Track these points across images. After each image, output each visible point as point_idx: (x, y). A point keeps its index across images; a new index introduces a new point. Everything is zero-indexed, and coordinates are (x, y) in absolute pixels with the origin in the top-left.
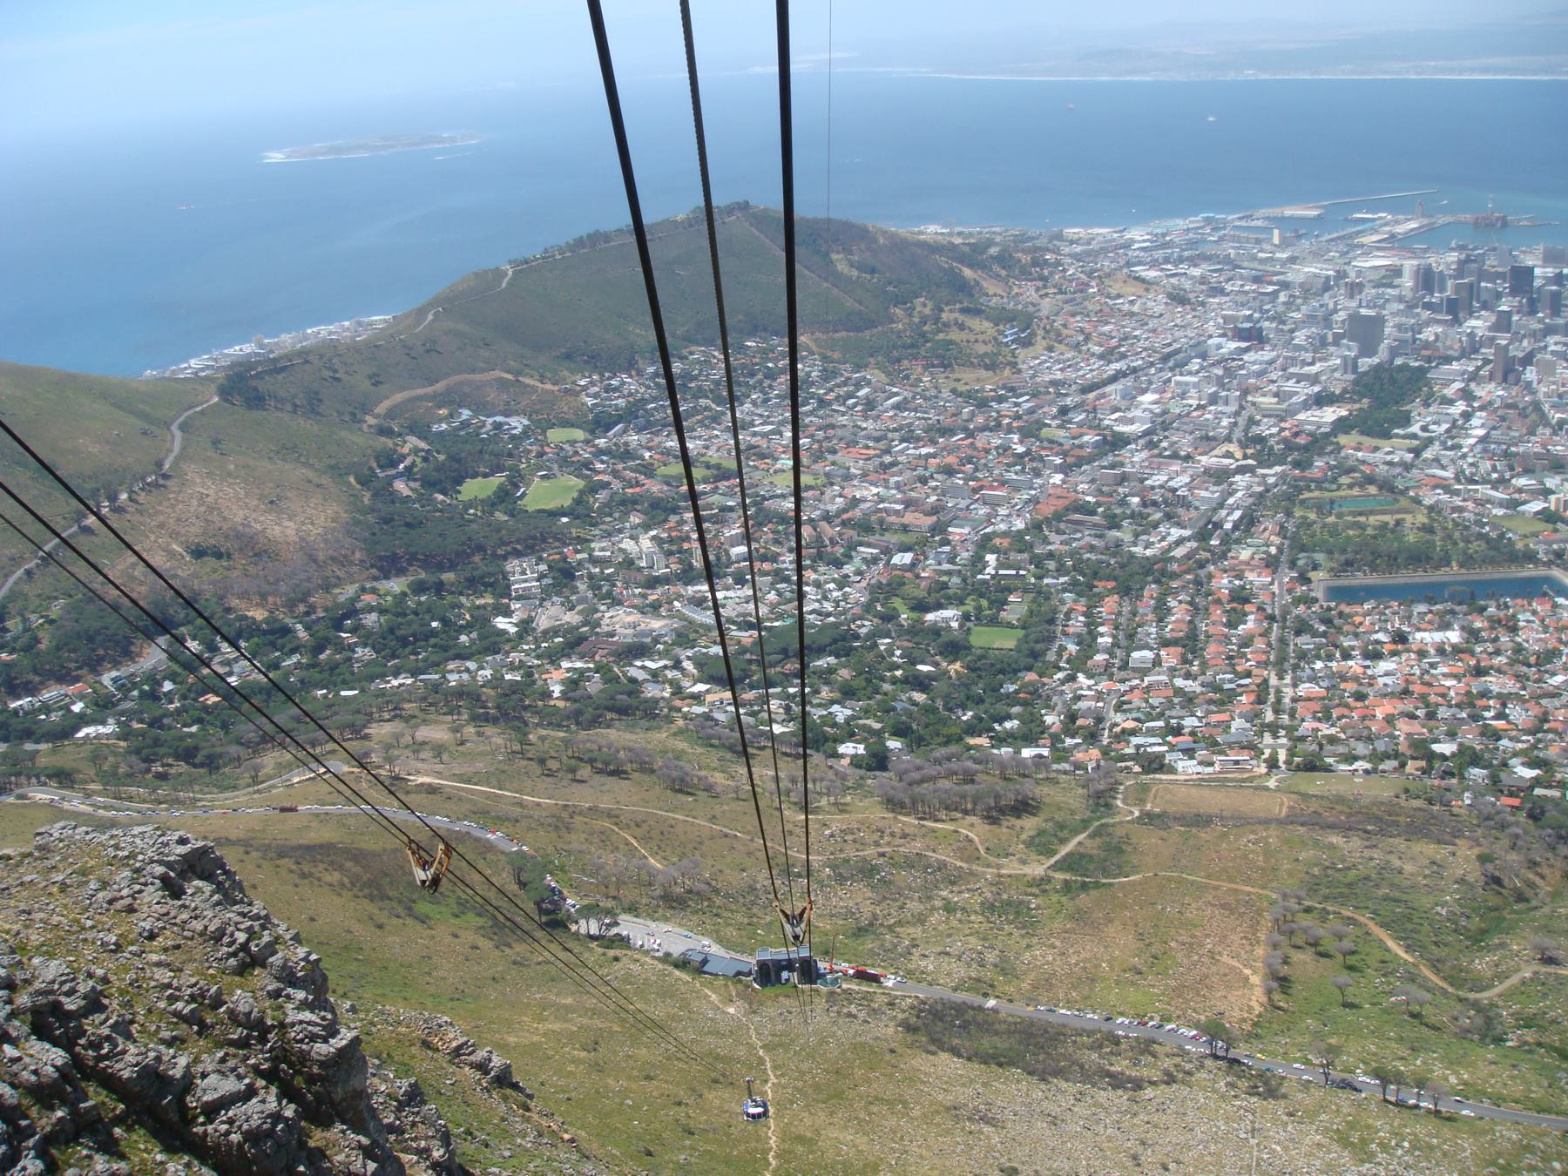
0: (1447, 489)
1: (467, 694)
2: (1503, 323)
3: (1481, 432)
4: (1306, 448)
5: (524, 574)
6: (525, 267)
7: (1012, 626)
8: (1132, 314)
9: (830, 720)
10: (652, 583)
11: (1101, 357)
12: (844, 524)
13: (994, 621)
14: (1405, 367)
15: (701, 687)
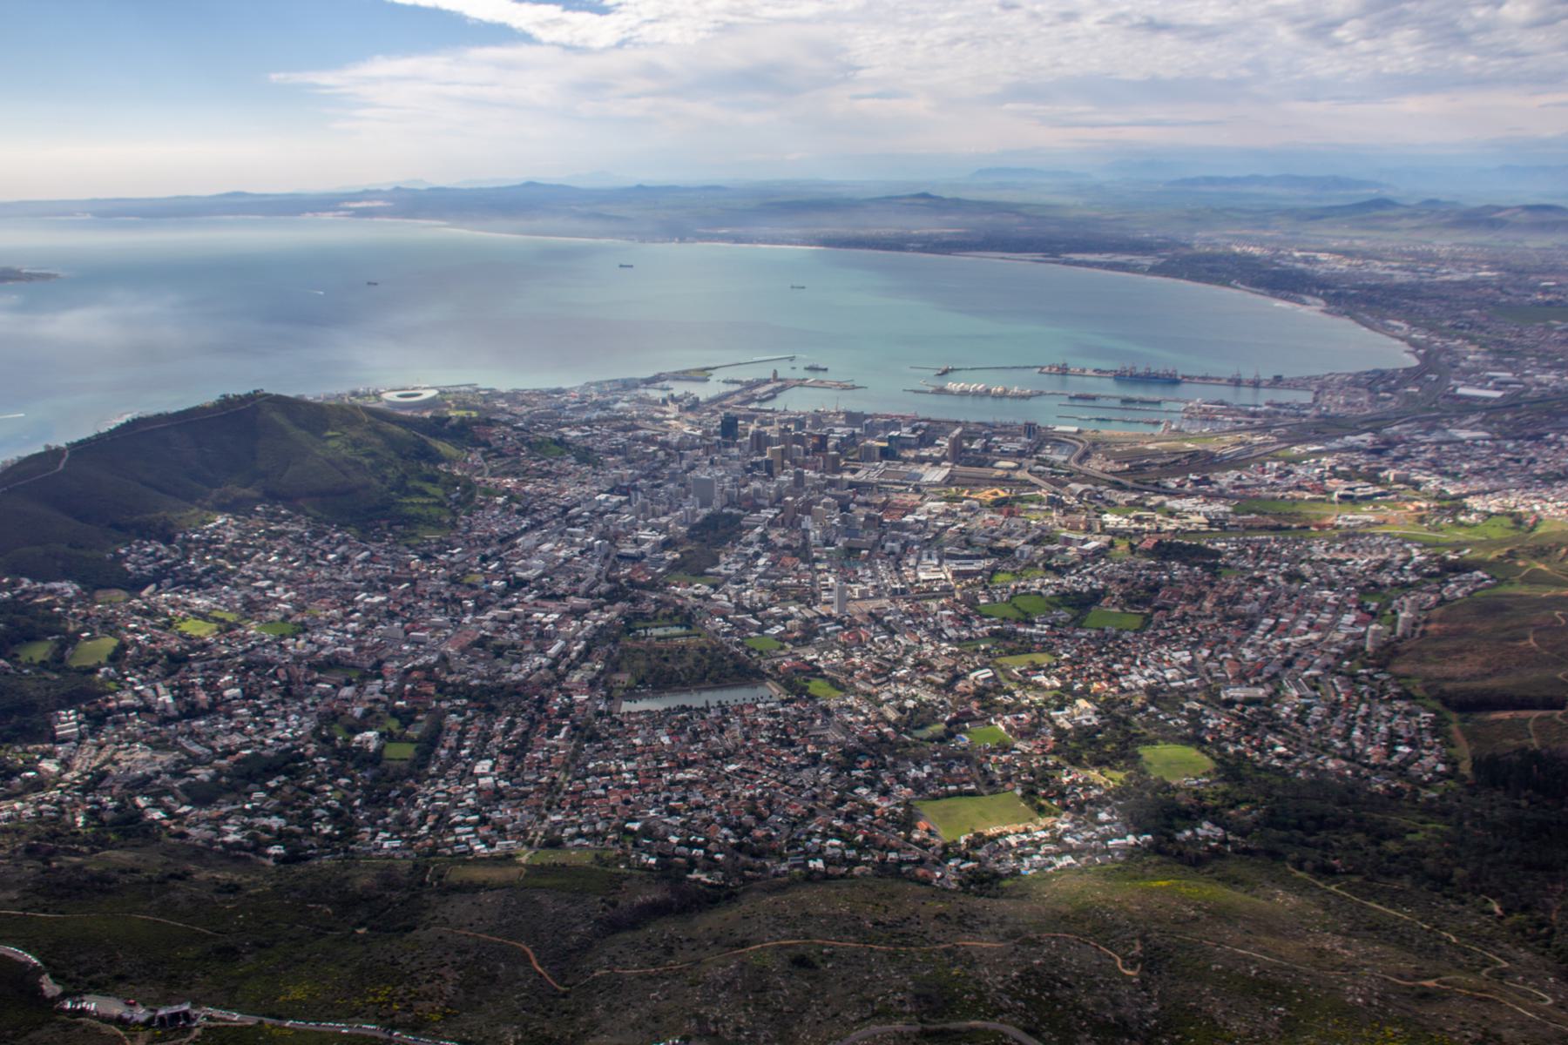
0: (726, 619)
1: (14, 828)
2: (799, 478)
3: (760, 570)
4: (643, 586)
5: (68, 722)
6: (82, 449)
7: (412, 741)
8: (548, 474)
9: (267, 829)
10: (166, 721)
11: (519, 512)
12: (311, 667)
13: (402, 739)
14: (730, 514)
15: (186, 809)
